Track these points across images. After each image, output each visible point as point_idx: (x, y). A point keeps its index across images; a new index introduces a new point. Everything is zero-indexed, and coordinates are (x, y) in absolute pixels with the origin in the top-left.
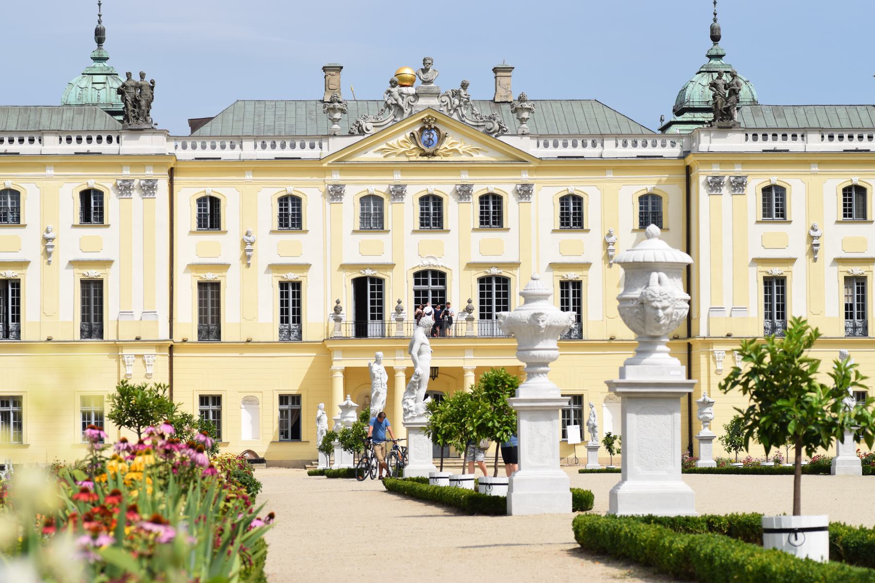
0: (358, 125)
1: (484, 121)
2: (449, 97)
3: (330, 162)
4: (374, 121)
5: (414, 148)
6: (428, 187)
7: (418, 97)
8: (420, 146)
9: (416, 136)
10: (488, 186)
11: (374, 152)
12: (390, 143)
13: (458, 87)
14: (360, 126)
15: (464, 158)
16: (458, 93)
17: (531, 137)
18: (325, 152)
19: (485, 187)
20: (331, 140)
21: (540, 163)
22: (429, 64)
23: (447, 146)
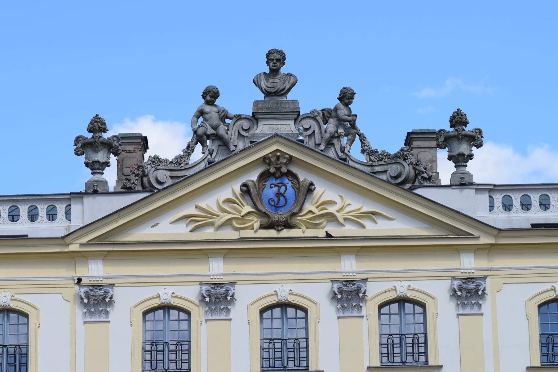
0: (140, 173)
1: (387, 164)
3: (85, 240)
4: (172, 167)
5: (249, 213)
6: (277, 288)
7: (257, 120)
8: (261, 208)
9: (252, 189)
10: (395, 284)
11: (172, 223)
13: (332, 102)
14: (145, 175)
15: (350, 230)
17: (476, 189)
18: (76, 223)
19: (389, 285)
20: (88, 200)
21: (496, 237)
22: (278, 60)
23: (313, 209)
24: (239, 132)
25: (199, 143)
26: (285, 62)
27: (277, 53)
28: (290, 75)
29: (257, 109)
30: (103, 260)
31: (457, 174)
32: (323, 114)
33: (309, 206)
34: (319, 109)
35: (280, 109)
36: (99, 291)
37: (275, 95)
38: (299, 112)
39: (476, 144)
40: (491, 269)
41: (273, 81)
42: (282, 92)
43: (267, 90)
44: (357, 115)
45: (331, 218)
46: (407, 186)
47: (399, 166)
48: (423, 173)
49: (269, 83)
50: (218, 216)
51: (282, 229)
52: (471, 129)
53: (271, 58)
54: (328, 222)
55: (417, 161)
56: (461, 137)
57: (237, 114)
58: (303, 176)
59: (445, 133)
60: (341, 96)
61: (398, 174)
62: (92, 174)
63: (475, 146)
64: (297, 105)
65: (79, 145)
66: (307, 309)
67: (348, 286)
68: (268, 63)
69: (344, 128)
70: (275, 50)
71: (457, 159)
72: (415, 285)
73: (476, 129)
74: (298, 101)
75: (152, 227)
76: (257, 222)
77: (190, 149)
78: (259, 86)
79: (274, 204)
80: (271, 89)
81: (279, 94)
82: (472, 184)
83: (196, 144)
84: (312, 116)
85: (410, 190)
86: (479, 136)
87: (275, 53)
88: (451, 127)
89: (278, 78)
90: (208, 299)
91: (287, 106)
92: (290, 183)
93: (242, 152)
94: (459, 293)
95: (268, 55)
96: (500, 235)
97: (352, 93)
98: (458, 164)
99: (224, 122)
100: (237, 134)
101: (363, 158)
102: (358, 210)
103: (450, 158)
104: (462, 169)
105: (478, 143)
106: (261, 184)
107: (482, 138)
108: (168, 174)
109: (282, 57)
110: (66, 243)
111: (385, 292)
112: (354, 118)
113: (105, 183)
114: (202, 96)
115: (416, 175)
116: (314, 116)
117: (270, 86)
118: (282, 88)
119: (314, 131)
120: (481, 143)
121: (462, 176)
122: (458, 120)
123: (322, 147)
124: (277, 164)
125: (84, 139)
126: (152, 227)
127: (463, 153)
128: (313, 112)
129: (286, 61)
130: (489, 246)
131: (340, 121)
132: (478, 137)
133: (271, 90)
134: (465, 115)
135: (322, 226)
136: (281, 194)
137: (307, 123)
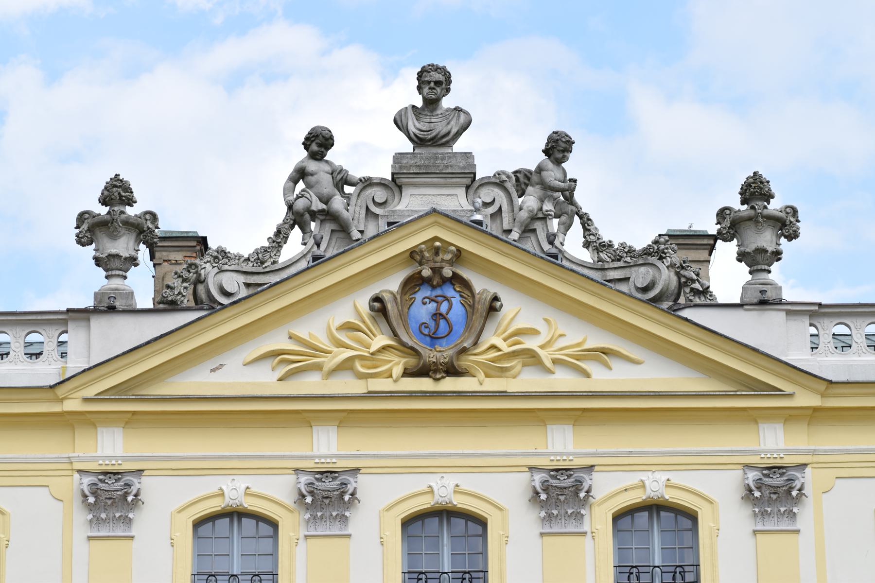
0: (192, 276)
2: (506, 190)
3: (91, 392)
4: (249, 267)
5: (385, 348)
6: (434, 481)
7: (400, 188)
8: (405, 338)
9: (389, 306)
10: (643, 476)
12: (302, 332)
14: (200, 281)
16: (535, 178)
17: (789, 313)
18: (76, 363)
19: (632, 479)
20: (98, 323)
21: (823, 395)
22: (438, 83)
23: (498, 341)
24: (367, 208)
25: (296, 226)
26: (450, 88)
27: (436, 70)
28: (459, 111)
29: (401, 168)
30: (123, 428)
31: (753, 285)
32: (517, 180)
33: (491, 338)
34: (510, 170)
35: (440, 168)
36: (114, 483)
37: (432, 144)
38: (475, 174)
39: (787, 234)
40: (814, 452)
41: (428, 120)
42: (445, 140)
43: (418, 135)
44: (576, 180)
45: (531, 358)
46: (665, 305)
47: (651, 271)
48: (693, 281)
49: (422, 123)
50: (329, 352)
51: (443, 377)
52: (778, 208)
53: (426, 79)
54: (524, 365)
55: (682, 262)
56: (760, 220)
57: (364, 176)
58: (481, 284)
59: (732, 213)
60: (549, 146)
61: (649, 284)
62: (107, 277)
63: (786, 237)
64: (470, 160)
65: (85, 227)
66: (486, 519)
67: (559, 479)
68: (419, 88)
69: (553, 203)
70: (433, 65)
71: (753, 259)
72: (677, 478)
73: (787, 207)
74: (473, 154)
75: (211, 372)
76: (398, 364)
77: (280, 237)
78: (403, 128)
79: (430, 332)
80: (425, 133)
81: (438, 143)
82: (780, 302)
83: (292, 227)
84: (498, 182)
85: (673, 310)
86: (792, 220)
87: (433, 71)
88: (743, 203)
89: (437, 115)
90: (309, 499)
91: (454, 162)
92: (457, 296)
93: (373, 240)
94: (757, 494)
95: (420, 74)
96: (830, 391)
97: (568, 141)
98: (755, 268)
99: (341, 191)
100: (364, 212)
101: (586, 256)
102: (578, 345)
103: (742, 257)
104: (763, 276)
105: (791, 231)
106: (407, 297)
107: (797, 224)
108: (242, 279)
109: (446, 79)
110: (58, 397)
111: (626, 490)
112: (571, 185)
113: (131, 295)
114: (303, 144)
115: (681, 286)
116: (500, 181)
117: (424, 128)
118: (445, 131)
119: (500, 208)
120: (795, 231)
121: (763, 287)
122: (755, 190)
123: (515, 235)
124: (435, 262)
125: (94, 217)
126: (213, 370)
127: (764, 248)
128: (499, 174)
129: (452, 86)
130: (811, 412)
131: (547, 188)
132: (790, 220)
133: (424, 135)
134: (768, 182)
135: (513, 372)
136: (441, 314)
137: (488, 192)
